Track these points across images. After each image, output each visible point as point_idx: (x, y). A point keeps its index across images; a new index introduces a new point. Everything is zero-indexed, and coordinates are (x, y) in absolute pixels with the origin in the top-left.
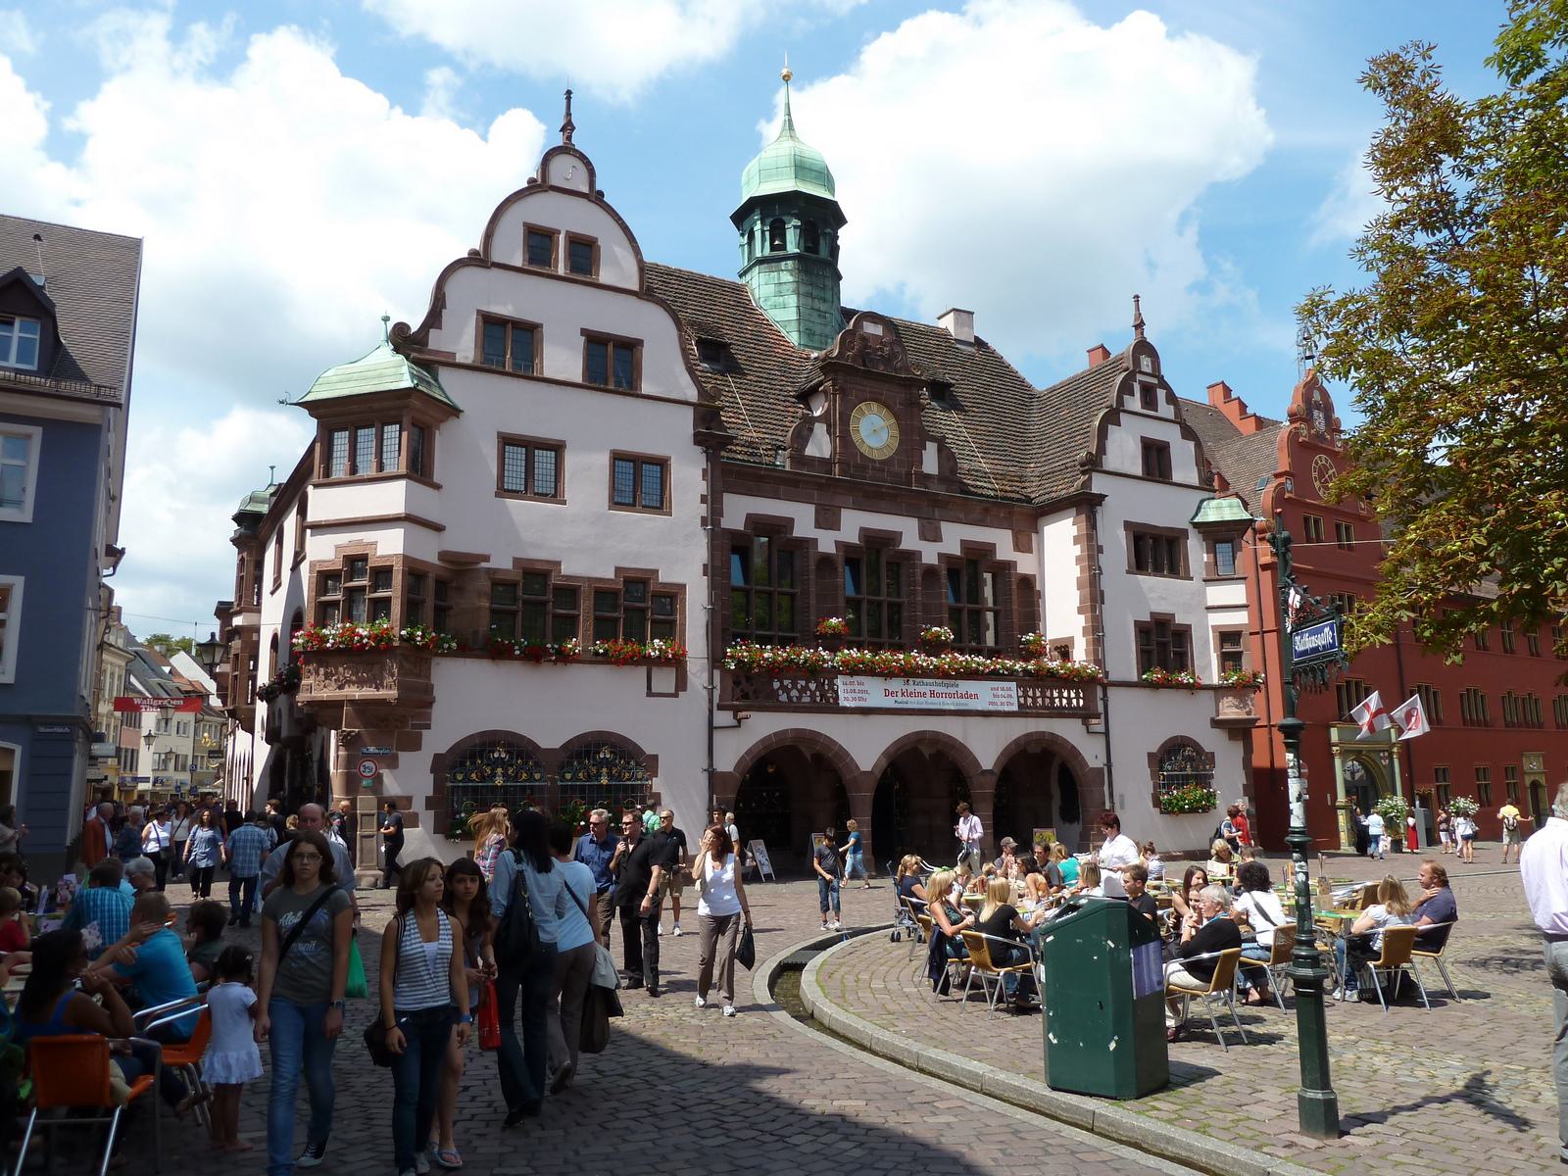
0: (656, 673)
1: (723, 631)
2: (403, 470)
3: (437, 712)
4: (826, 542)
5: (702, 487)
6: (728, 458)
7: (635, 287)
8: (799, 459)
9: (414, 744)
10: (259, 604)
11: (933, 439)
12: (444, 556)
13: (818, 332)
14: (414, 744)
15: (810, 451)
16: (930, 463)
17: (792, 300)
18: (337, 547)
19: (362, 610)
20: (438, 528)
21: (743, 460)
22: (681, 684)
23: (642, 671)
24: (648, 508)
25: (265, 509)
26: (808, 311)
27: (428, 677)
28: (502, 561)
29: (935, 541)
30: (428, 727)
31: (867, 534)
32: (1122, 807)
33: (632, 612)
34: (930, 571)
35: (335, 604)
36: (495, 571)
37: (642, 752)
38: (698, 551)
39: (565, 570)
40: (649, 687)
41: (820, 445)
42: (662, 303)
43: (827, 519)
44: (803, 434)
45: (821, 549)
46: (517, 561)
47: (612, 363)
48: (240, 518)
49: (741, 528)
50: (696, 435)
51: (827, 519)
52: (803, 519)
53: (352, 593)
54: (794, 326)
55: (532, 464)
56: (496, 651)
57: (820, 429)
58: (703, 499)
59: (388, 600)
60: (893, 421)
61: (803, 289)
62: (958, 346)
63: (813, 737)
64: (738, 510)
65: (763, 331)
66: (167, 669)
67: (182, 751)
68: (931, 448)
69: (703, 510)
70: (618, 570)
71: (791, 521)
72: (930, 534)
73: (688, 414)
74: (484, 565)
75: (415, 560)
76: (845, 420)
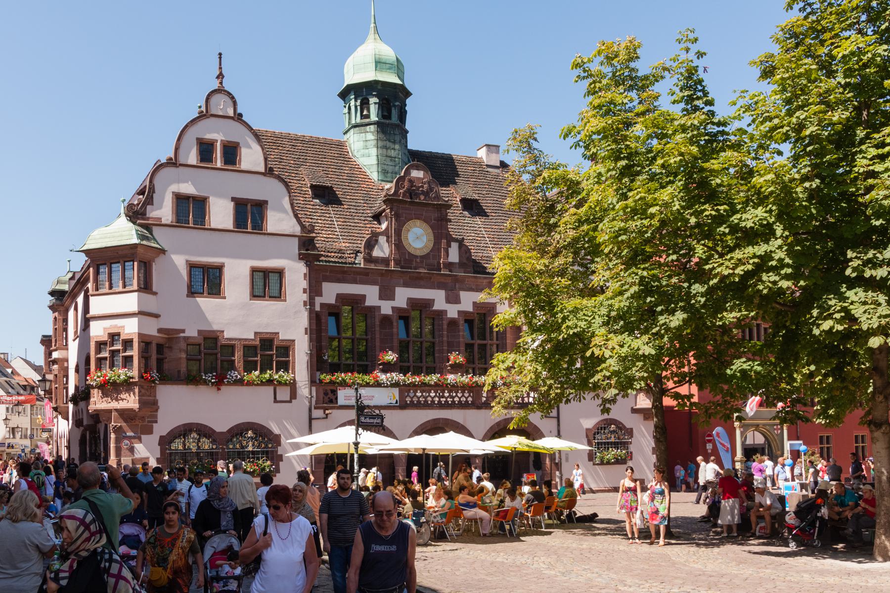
0: (279, 390)
1: (318, 363)
2: (135, 287)
3: (160, 414)
4: (386, 308)
5: (304, 284)
6: (326, 261)
7: (263, 171)
8: (369, 259)
9: (149, 431)
10: (67, 345)
11: (456, 240)
12: (160, 331)
13: (390, 171)
14: (149, 431)
15: (376, 253)
16: (454, 255)
17: (374, 151)
18: (104, 329)
19: (119, 360)
20: (157, 316)
21: (335, 262)
22: (293, 395)
23: (271, 388)
24: (272, 297)
25: (66, 287)
26: (384, 158)
27: (155, 396)
28: (192, 332)
29: (456, 303)
30: (156, 422)
31: (412, 302)
32: (567, 460)
33: (269, 352)
34: (453, 323)
35: (105, 358)
36: (188, 338)
38: (303, 320)
39: (227, 335)
40: (275, 398)
41: (383, 250)
42: (279, 178)
43: (387, 294)
44: (371, 244)
45: (383, 312)
46: (200, 332)
47: (249, 215)
48: (53, 293)
49: (333, 301)
50: (300, 254)
51: (387, 294)
52: (371, 294)
53: (114, 353)
54: (375, 168)
55: (207, 279)
56: (192, 379)
57: (382, 240)
58: (305, 291)
59: (132, 357)
60: (430, 230)
61: (380, 144)
62: (489, 169)
64: (331, 292)
65: (356, 173)
66: (9, 371)
67: (24, 426)
68: (455, 246)
69: (305, 297)
71: (364, 297)
72: (453, 299)
73: (296, 240)
74: (182, 335)
75: (145, 335)
76: (398, 233)
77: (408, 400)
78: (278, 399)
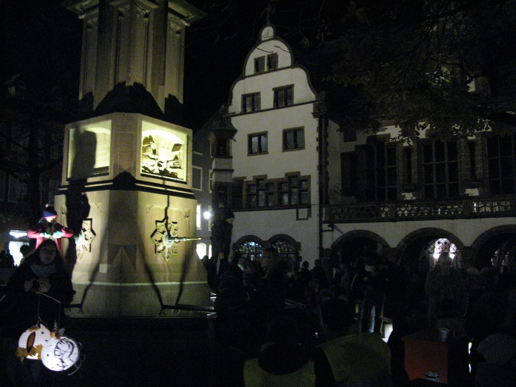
22: (309, 215)
28: (250, 178)
37: (294, 240)
39: (269, 177)
40: (297, 217)
63: (368, 232)
70: (286, 174)
74: (245, 180)
77: (400, 213)
78: (300, 217)
